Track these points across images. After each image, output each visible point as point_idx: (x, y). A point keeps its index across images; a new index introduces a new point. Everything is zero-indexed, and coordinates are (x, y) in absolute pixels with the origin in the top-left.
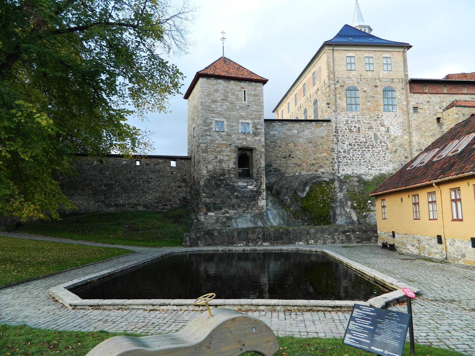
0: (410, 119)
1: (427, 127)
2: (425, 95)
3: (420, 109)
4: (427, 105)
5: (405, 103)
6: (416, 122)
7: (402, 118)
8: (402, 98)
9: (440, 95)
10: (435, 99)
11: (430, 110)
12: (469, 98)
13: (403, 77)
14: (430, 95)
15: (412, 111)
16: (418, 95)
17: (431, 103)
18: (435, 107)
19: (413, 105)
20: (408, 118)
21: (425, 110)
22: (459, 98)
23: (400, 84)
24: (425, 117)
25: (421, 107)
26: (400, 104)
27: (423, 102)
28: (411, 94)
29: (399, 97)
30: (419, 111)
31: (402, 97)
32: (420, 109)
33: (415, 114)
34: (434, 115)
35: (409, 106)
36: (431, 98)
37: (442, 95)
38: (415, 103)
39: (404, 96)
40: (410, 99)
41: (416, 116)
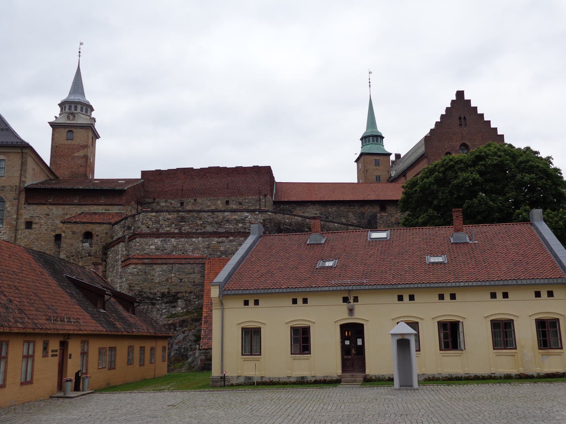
0: (19, 236)
1: (40, 246)
2: (45, 207)
3: (35, 223)
4: (44, 219)
5: (15, 216)
6: (26, 240)
7: (8, 235)
8: (13, 211)
9: (64, 206)
10: (57, 211)
11: (47, 225)
12: (103, 209)
13: (18, 184)
14: (50, 207)
15: (23, 226)
16: (35, 206)
17: (51, 216)
18: (55, 221)
19: (25, 219)
20: (16, 236)
21: (41, 225)
22: (90, 210)
23: (13, 192)
24: (39, 234)
25: (37, 220)
26: (9, 218)
27: (40, 216)
28: (25, 206)
29: (9, 209)
30: (34, 226)
31: (12, 209)
32: (36, 223)
33: (27, 230)
34: (51, 231)
35: (20, 221)
36: (52, 210)
37: (67, 207)
38: (28, 217)
39: (15, 208)
40: (22, 211)
41: (27, 233)
